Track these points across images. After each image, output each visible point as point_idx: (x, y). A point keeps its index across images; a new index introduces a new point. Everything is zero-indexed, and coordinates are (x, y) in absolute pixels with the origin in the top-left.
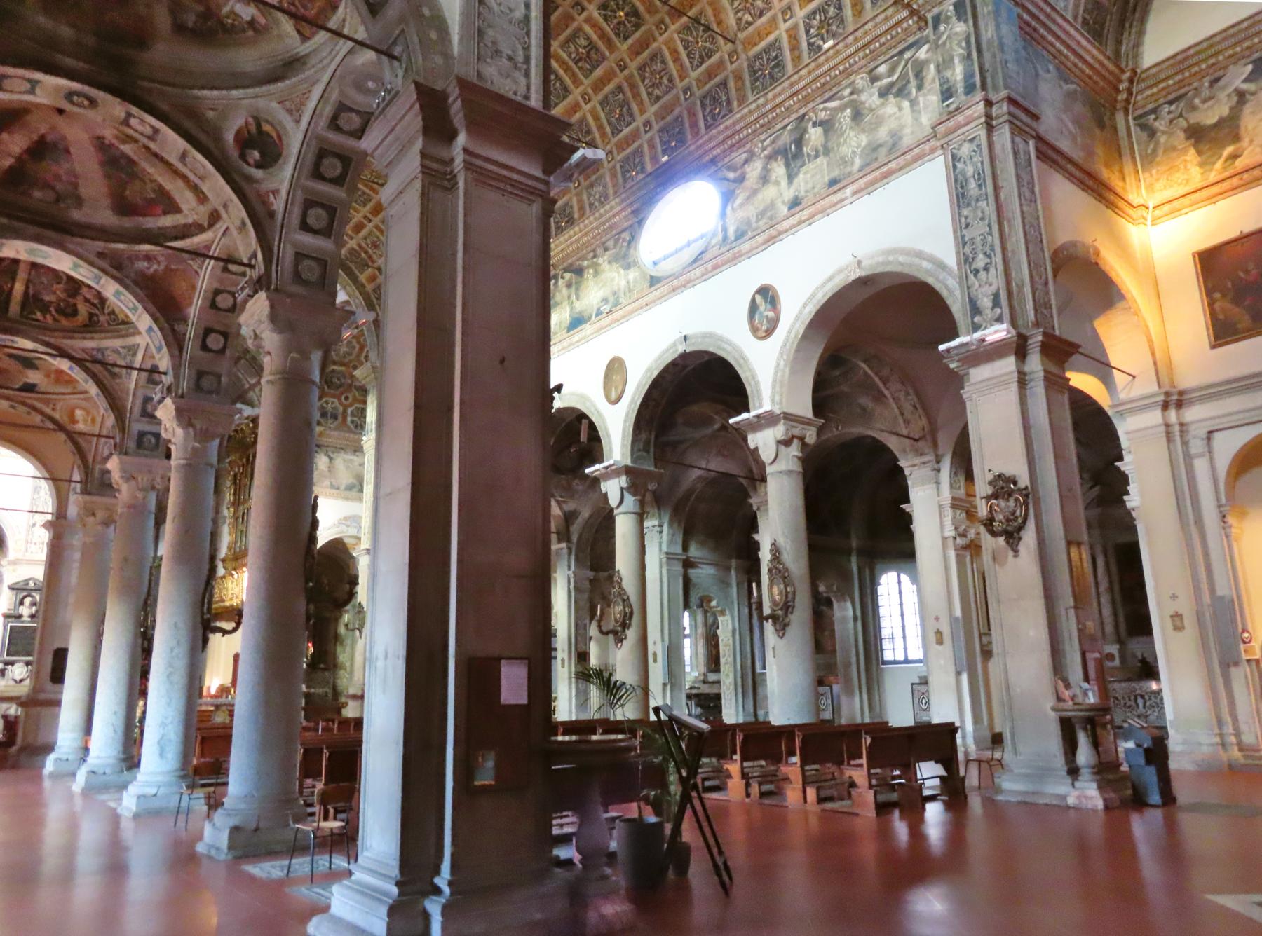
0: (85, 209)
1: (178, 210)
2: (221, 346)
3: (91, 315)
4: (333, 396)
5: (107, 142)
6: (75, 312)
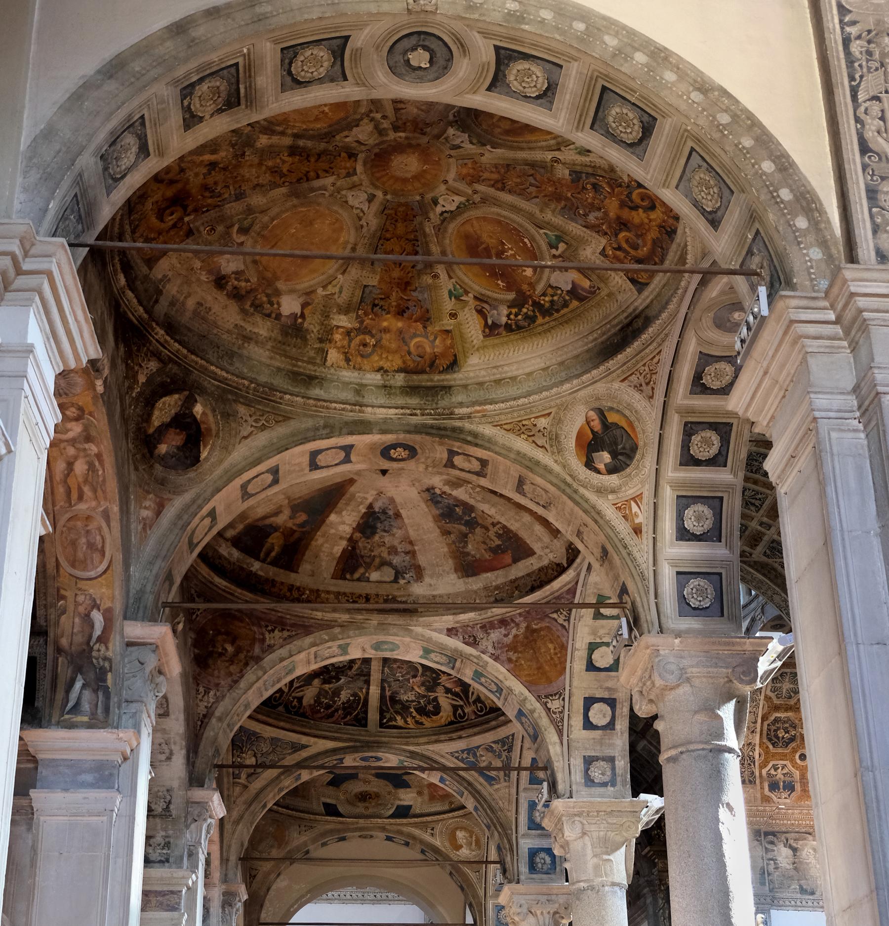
0: (427, 580)
1: (530, 553)
2: (608, 719)
3: (455, 708)
4: (783, 757)
5: (438, 491)
6: (437, 710)
